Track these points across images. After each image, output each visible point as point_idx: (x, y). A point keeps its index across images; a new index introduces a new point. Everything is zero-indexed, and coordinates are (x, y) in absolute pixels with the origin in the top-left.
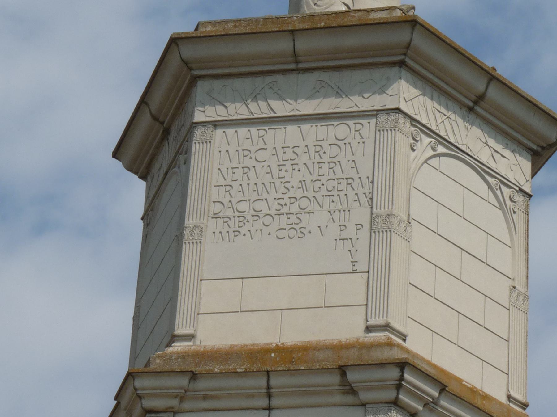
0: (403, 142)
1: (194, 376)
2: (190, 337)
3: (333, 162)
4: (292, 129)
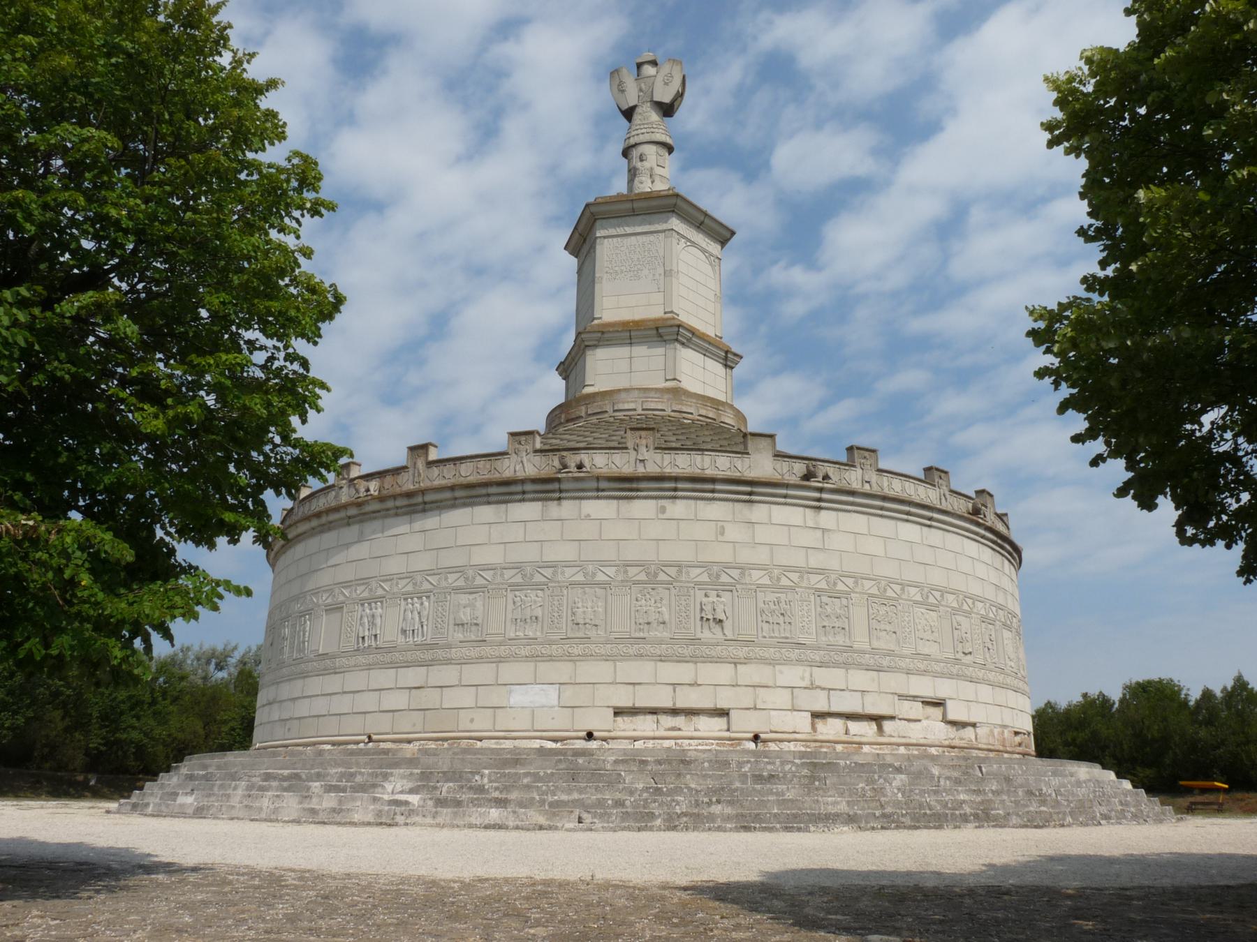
0: (675, 241)
1: (603, 333)
2: (600, 318)
3: (649, 250)
4: (633, 238)
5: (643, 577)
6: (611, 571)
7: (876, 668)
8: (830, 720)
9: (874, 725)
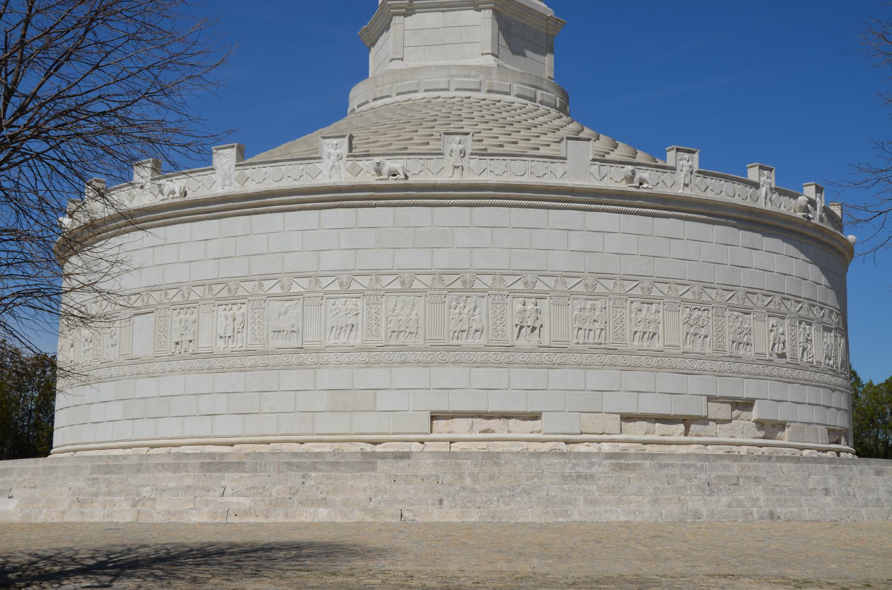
5: (459, 285)
6: (427, 279)
7: (686, 371)
8: (638, 423)
9: (681, 427)
